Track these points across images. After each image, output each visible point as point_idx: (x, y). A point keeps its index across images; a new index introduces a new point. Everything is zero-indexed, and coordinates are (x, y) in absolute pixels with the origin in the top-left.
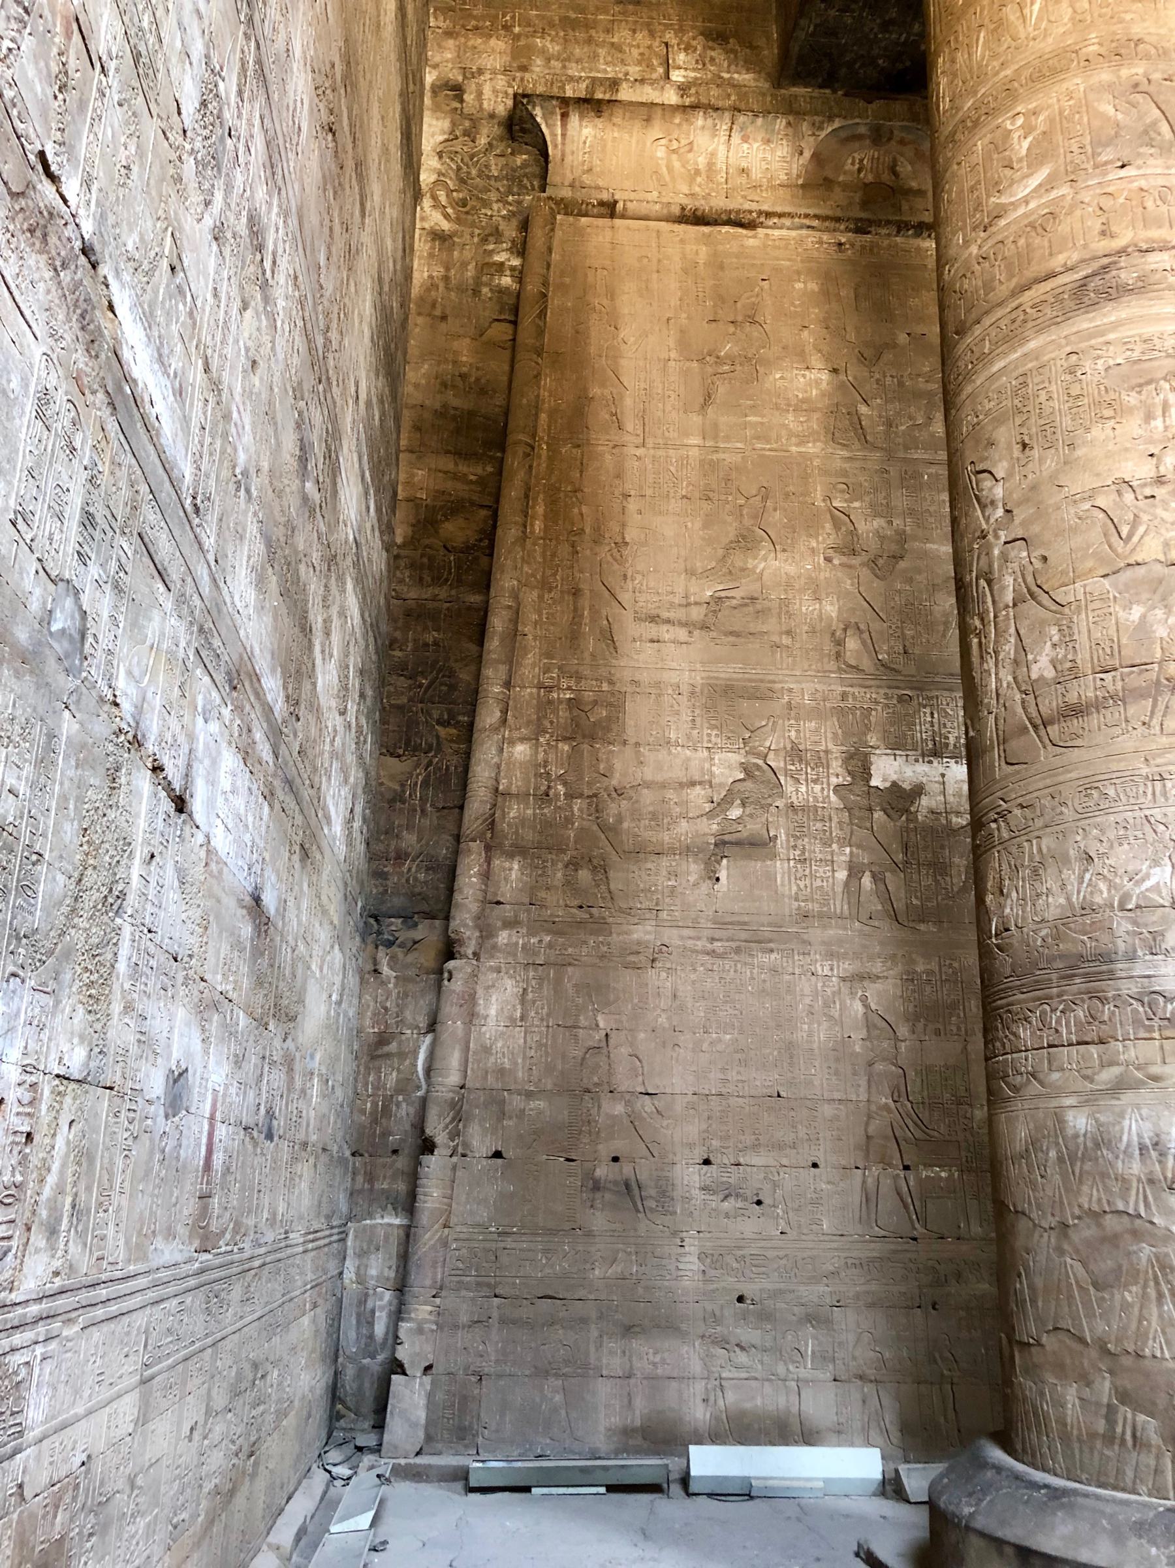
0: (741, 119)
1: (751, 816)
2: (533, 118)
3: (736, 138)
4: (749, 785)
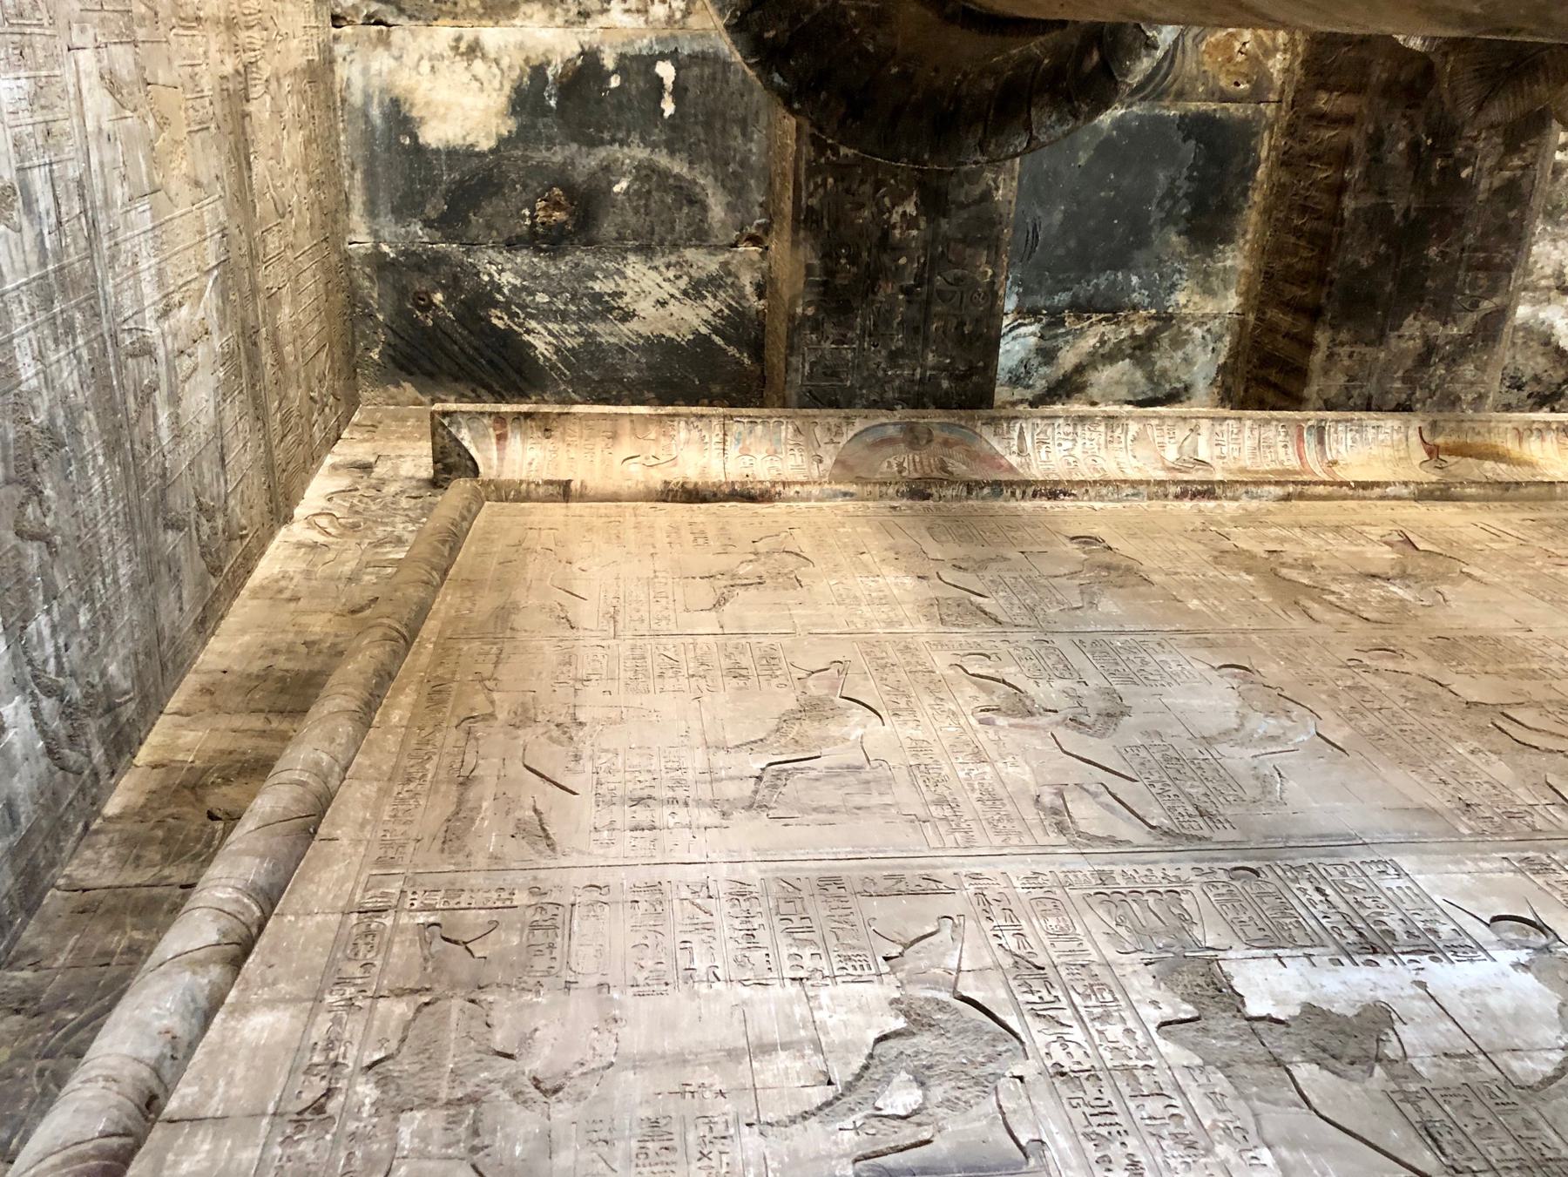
0: (736, 428)
1: (950, 1103)
3: (733, 451)
4: (925, 1041)
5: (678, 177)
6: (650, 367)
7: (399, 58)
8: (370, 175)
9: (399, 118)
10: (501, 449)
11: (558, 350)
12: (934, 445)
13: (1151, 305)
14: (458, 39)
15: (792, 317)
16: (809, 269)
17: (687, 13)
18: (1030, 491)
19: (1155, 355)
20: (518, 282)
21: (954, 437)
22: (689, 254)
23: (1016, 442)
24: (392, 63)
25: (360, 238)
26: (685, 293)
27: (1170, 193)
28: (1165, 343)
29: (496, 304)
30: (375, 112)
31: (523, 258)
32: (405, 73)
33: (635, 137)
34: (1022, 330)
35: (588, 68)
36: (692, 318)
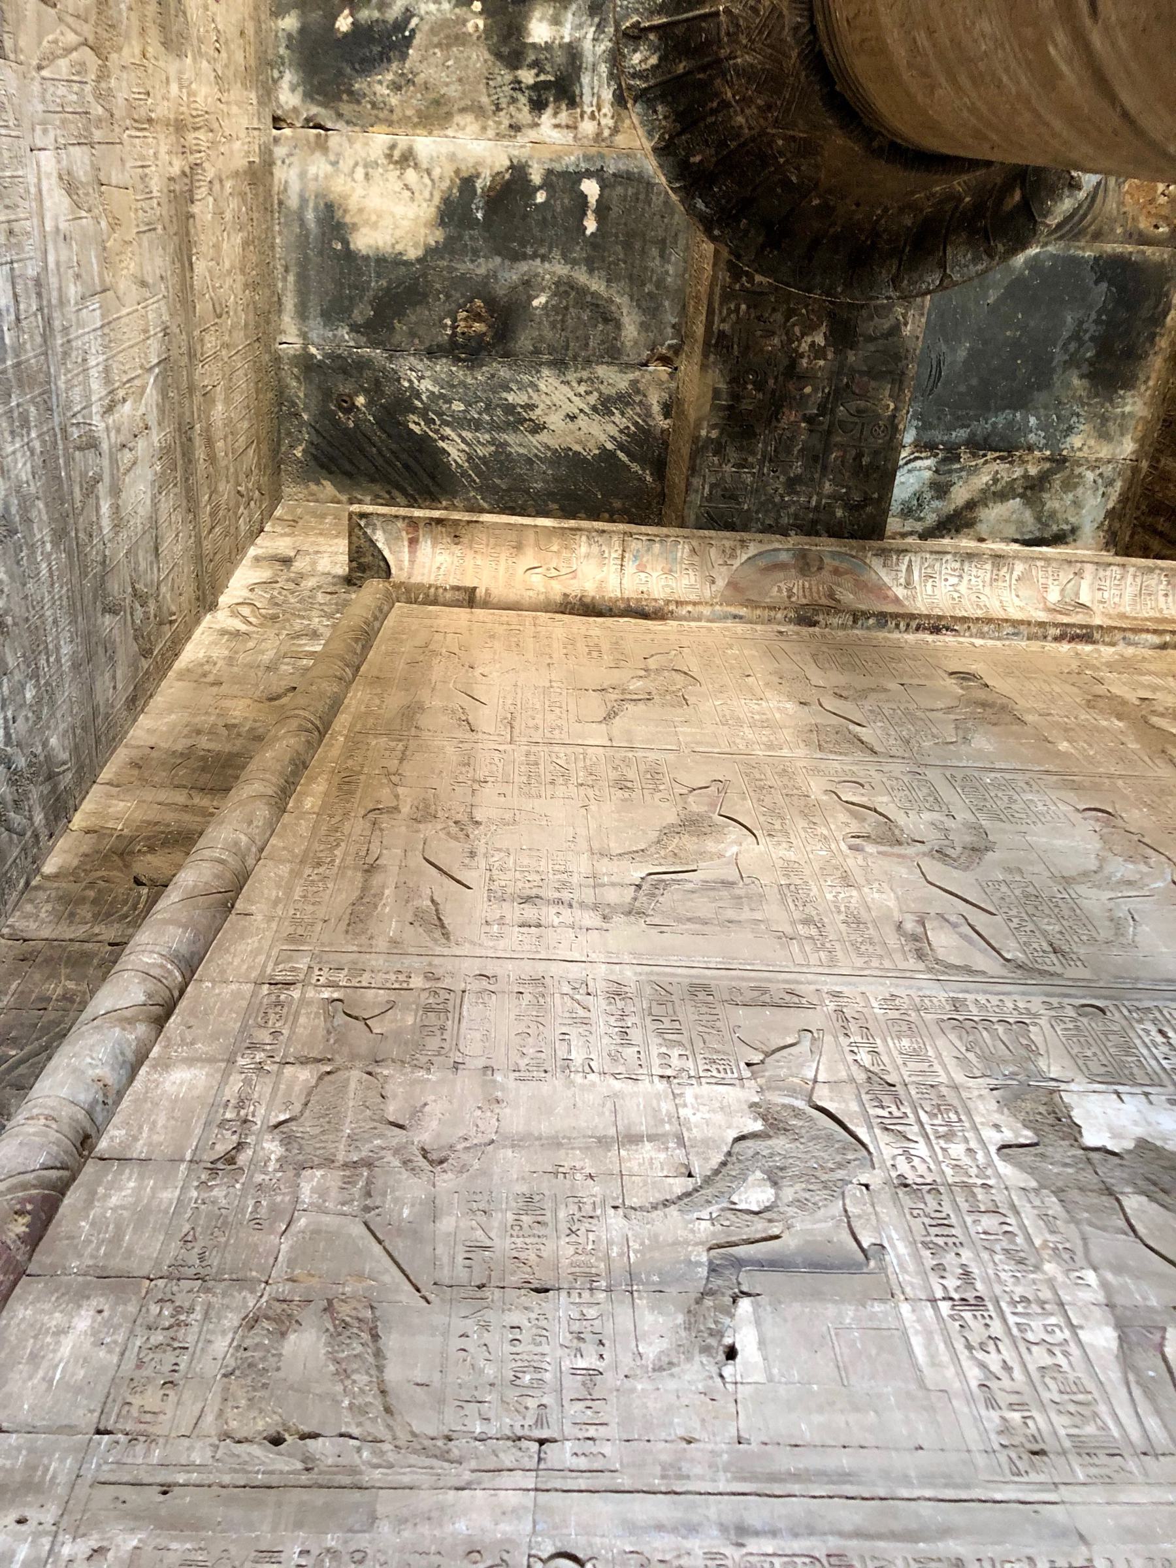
0: (634, 545)
1: (800, 1203)
2: (373, 543)
3: (630, 567)
4: (780, 1143)
5: (594, 294)
6: (556, 479)
7: (335, 164)
8: (302, 278)
9: (333, 222)
10: (413, 551)
11: (470, 458)
12: (825, 574)
13: (1046, 446)
14: (393, 147)
15: (696, 439)
16: (716, 393)
17: (615, 131)
18: (914, 624)
19: (1046, 496)
20: (436, 390)
22: (601, 371)
23: (903, 574)
24: (329, 168)
25: (290, 338)
26: (594, 409)
27: (1076, 336)
28: (1057, 484)
29: (414, 410)
30: (310, 216)
31: (442, 367)
32: (341, 180)
33: (556, 254)
34: (918, 463)
35: (513, 186)
36: (599, 433)
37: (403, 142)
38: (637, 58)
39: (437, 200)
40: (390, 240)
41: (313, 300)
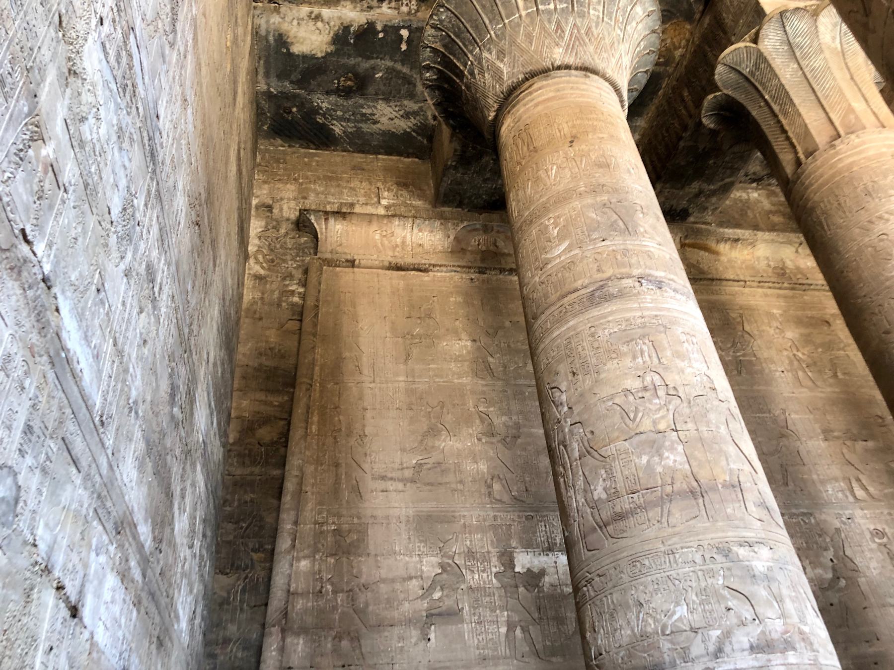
0: (418, 221)
1: (447, 596)
2: (310, 220)
3: (415, 231)
4: (445, 576)
5: (404, 74)
6: (384, 141)
7: (283, 18)
8: (267, 62)
9: (282, 41)
10: (326, 224)
11: (344, 132)
14: (311, 13)
15: (446, 165)
16: (456, 150)
17: (417, 11)
20: (330, 107)
21: (501, 230)
22: (406, 102)
24: (280, 20)
25: (262, 86)
26: (402, 116)
29: (319, 114)
30: (271, 38)
31: (333, 98)
32: (286, 24)
33: (387, 57)
35: (369, 29)
36: (404, 125)
37: (316, 10)
38: (428, 75)
39: (332, 34)
40: (309, 49)
41: (272, 71)
